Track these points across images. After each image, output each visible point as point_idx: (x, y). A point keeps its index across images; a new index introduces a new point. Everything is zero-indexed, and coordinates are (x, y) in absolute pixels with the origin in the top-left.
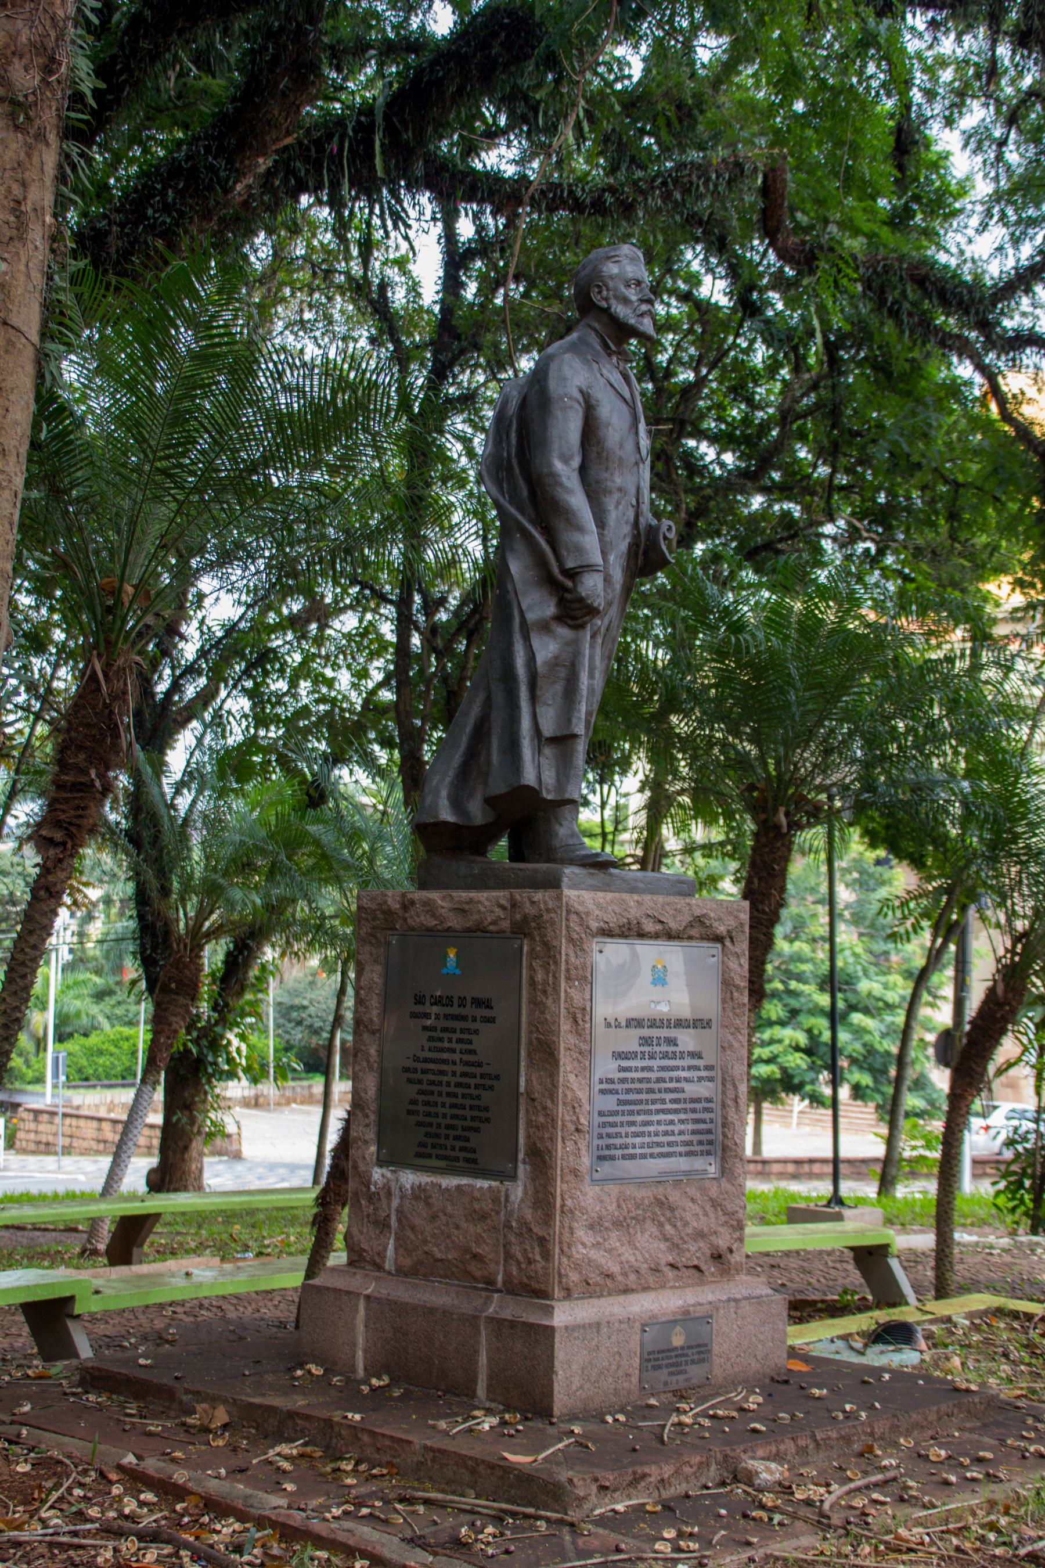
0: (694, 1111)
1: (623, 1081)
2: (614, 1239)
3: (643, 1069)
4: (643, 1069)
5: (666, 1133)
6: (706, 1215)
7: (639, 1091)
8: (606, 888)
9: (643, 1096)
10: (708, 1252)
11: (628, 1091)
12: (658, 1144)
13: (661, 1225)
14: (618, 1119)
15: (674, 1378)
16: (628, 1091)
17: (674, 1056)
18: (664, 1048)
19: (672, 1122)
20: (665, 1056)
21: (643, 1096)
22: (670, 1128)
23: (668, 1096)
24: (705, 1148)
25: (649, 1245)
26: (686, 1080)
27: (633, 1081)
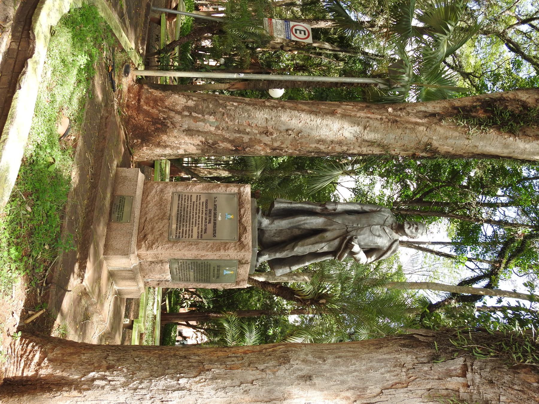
0: (189, 231)
1: (200, 203)
2: (157, 198)
3: (202, 211)
4: (202, 211)
5: (184, 219)
6: (159, 231)
7: (196, 210)
8: (252, 214)
9: (195, 211)
10: (147, 233)
11: (197, 205)
12: (181, 216)
13: (158, 215)
14: (189, 202)
15: (115, 207)
16: (197, 205)
17: (206, 222)
18: (208, 219)
19: (187, 222)
20: (206, 219)
21: (195, 211)
22: (185, 221)
23: (194, 220)
24: (178, 235)
25: (153, 211)
26: (198, 227)
27: (199, 207)
